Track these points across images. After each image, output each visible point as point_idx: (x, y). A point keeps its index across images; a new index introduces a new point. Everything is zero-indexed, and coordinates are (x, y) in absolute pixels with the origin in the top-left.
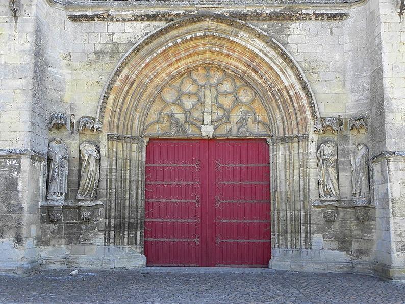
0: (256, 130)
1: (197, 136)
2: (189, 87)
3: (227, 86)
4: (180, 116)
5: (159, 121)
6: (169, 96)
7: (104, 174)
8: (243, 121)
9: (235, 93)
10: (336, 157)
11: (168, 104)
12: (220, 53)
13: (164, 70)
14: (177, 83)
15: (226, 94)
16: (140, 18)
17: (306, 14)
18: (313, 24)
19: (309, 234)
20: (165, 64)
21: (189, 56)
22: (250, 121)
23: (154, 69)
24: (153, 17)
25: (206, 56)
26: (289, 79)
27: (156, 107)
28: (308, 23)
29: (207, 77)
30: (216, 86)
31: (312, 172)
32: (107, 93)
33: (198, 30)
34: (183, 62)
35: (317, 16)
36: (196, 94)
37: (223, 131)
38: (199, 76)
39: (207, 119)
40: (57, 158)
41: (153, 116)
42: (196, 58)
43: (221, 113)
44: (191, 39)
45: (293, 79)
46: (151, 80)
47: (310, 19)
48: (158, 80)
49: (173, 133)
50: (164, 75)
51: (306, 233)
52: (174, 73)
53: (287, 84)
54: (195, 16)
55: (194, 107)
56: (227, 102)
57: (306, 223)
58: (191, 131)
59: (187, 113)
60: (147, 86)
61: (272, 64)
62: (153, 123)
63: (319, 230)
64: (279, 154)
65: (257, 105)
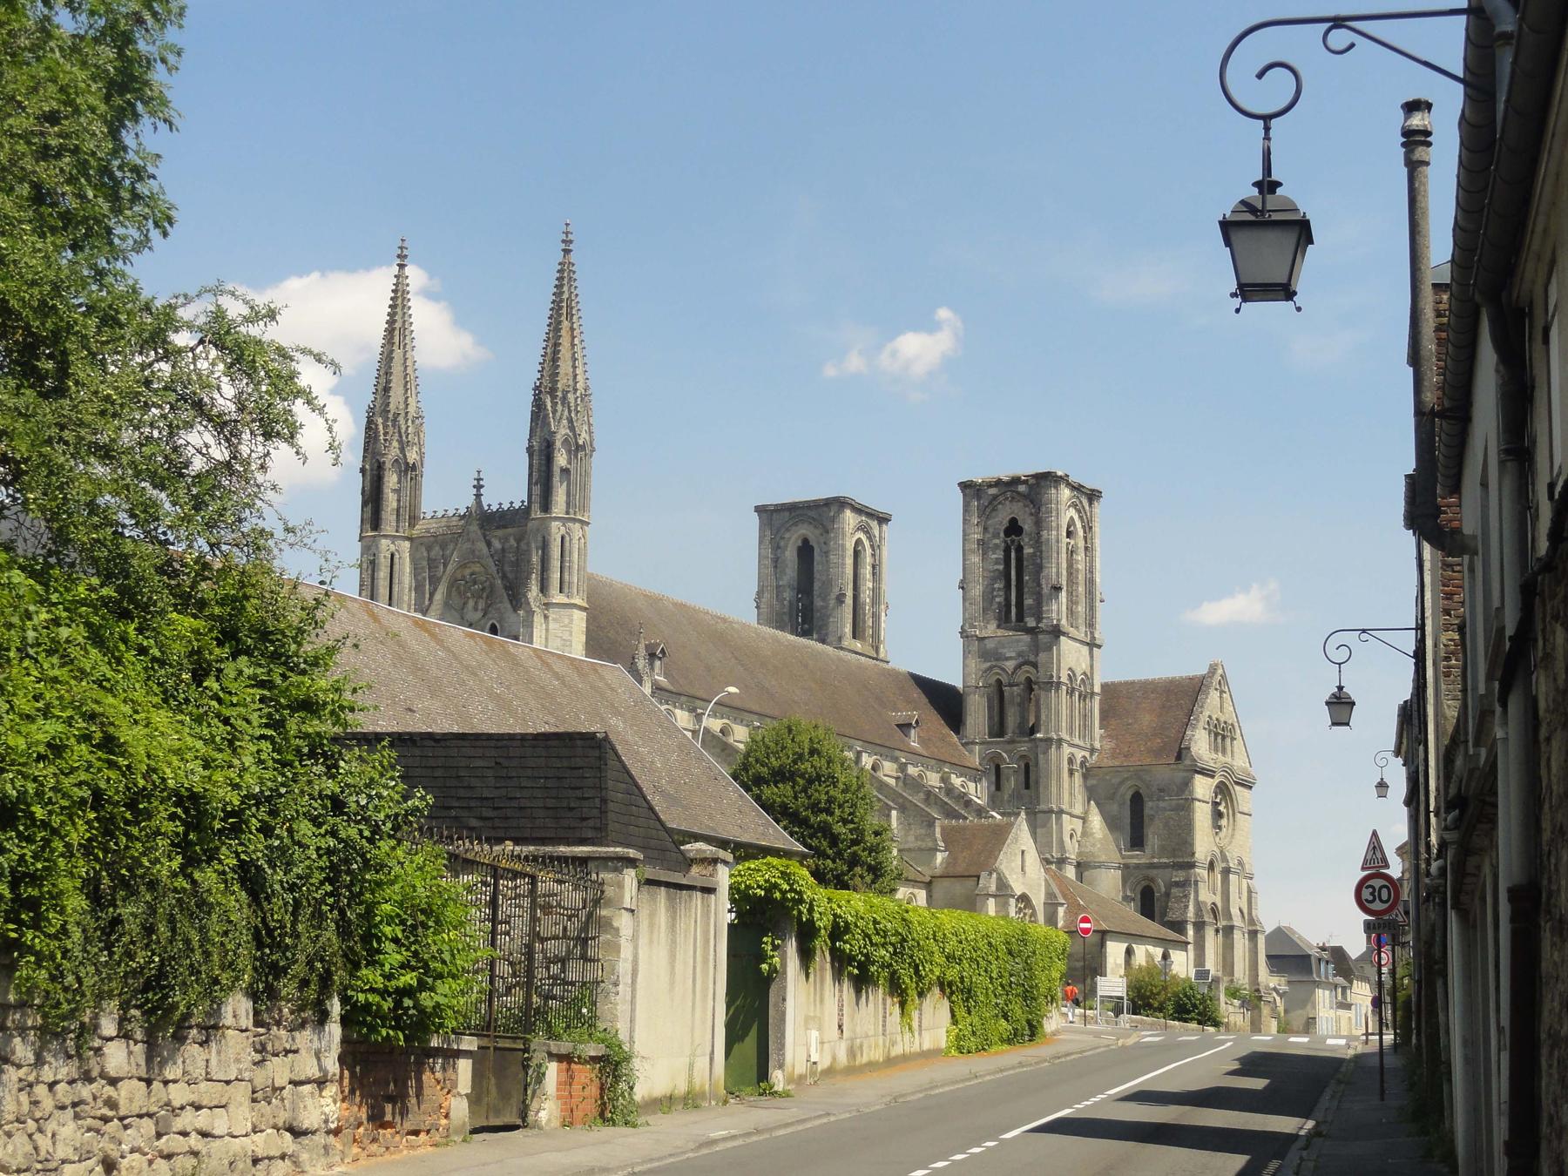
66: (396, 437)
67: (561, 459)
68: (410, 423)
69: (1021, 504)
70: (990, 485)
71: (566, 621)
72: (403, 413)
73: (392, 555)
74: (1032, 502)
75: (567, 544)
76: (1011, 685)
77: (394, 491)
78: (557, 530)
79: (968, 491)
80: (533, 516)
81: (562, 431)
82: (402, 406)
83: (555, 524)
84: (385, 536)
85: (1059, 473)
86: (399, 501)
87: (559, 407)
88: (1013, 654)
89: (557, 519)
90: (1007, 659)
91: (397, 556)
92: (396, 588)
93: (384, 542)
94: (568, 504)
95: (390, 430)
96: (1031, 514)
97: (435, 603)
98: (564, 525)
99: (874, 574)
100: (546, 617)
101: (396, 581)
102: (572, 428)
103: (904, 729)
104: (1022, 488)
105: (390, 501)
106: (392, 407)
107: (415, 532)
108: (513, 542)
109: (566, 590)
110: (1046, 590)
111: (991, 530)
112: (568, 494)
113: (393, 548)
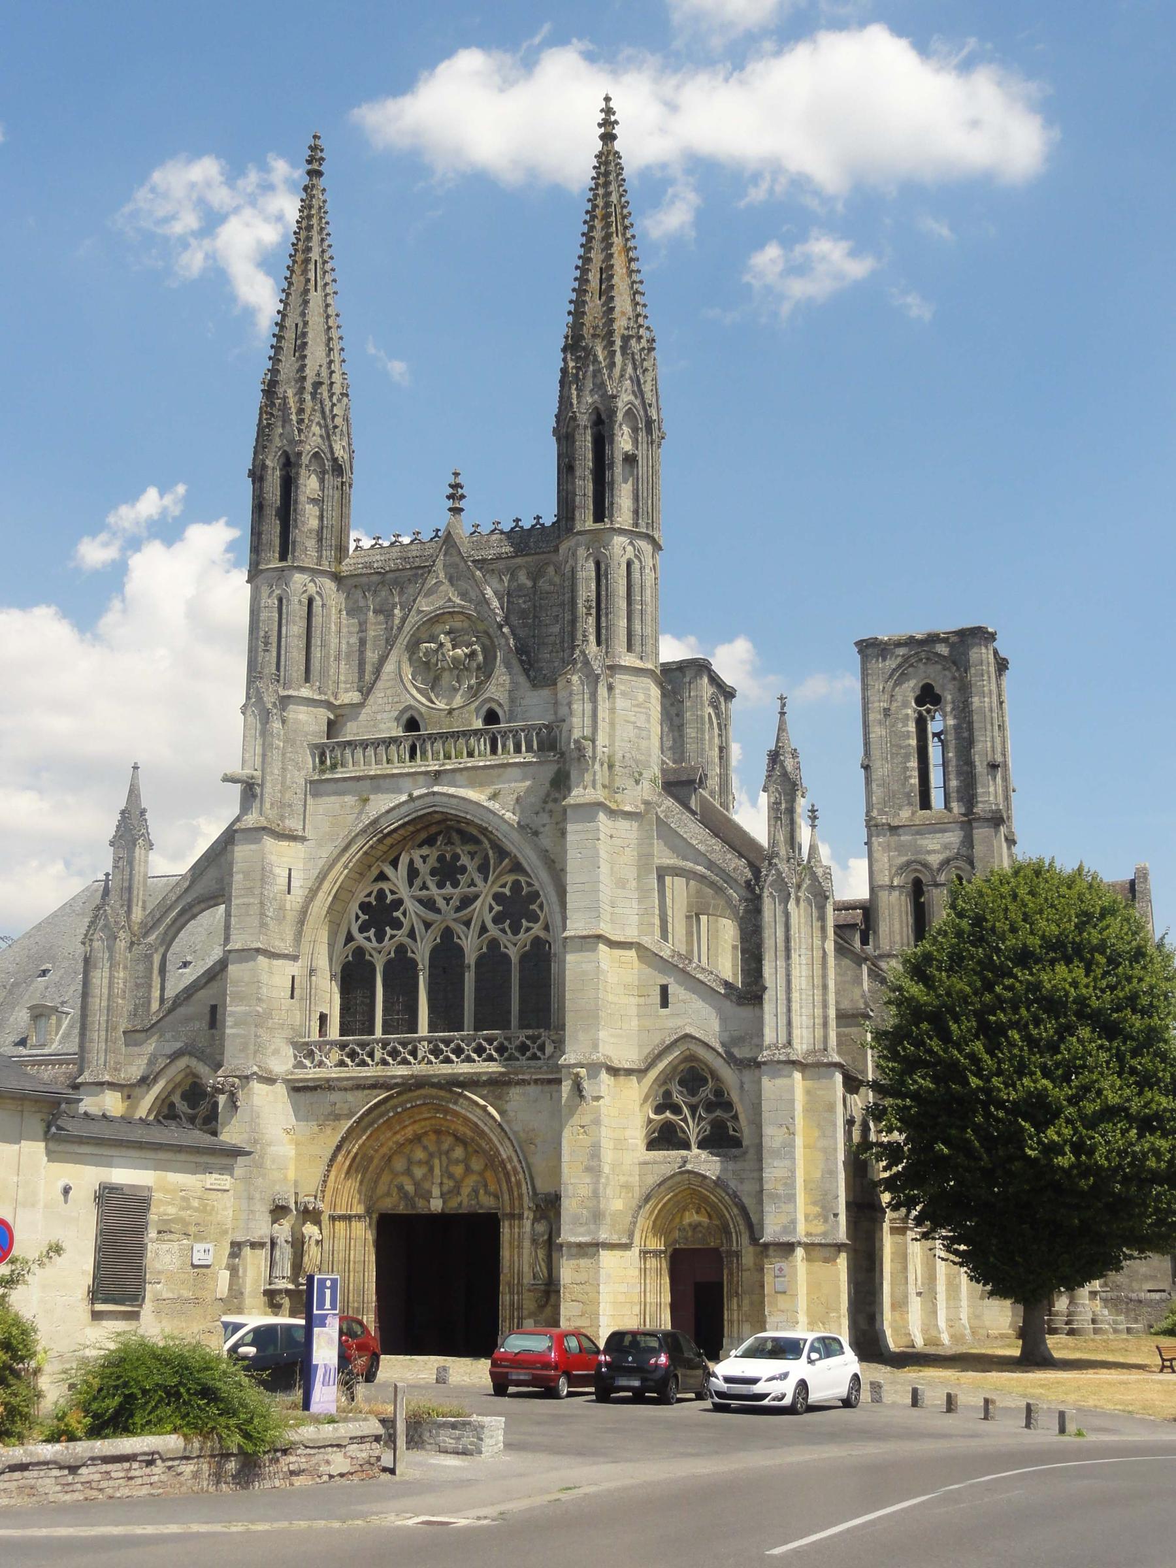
0: (487, 1203)
1: (426, 1211)
2: (420, 1154)
3: (459, 1152)
4: (410, 1188)
5: (388, 1194)
6: (399, 1164)
7: (326, 1255)
8: (475, 1191)
9: (466, 1162)
10: (546, 1237)
11: (396, 1174)
12: (445, 1119)
13: (389, 1139)
14: (407, 1150)
15: (457, 1162)
16: (359, 1087)
17: (523, 1080)
18: (531, 1089)
19: (520, 1319)
20: (389, 1134)
21: (415, 1122)
22: (482, 1192)
23: (377, 1139)
24: (374, 1086)
25: (433, 1122)
26: (505, 1152)
27: (386, 1178)
28: (528, 1088)
29: (439, 1142)
30: (447, 1153)
31: (526, 1252)
32: (328, 1171)
33: (418, 1098)
34: (409, 1128)
35: (536, 1081)
36: (427, 1163)
37: (453, 1204)
38: (430, 1141)
39: (436, 1191)
40: (280, 1241)
41: (382, 1188)
42: (423, 1123)
43: (451, 1184)
44: (412, 1107)
45: (511, 1152)
46: (376, 1151)
47: (529, 1084)
48: (384, 1150)
49: (402, 1209)
50: (390, 1143)
51: (519, 1318)
52: (401, 1141)
53: (504, 1156)
54: (412, 1085)
55: (425, 1176)
56: (458, 1170)
57: (518, 1308)
58: (421, 1207)
59: (417, 1185)
60: (371, 1159)
61: (491, 1135)
62: (382, 1197)
63: (530, 1316)
64: (505, 1230)
65: (489, 1175)
66: (317, 417)
67: (624, 442)
68: (335, 400)
69: (939, 667)
70: (899, 644)
71: (641, 698)
72: (327, 382)
73: (311, 601)
74: (954, 663)
75: (636, 575)
76: (937, 885)
77: (313, 501)
78: (620, 548)
79: (870, 651)
80: (578, 527)
81: (625, 399)
82: (324, 373)
83: (619, 541)
84: (301, 569)
85: (990, 630)
86: (321, 518)
87: (618, 358)
88: (938, 847)
89: (622, 531)
90: (929, 852)
91: (318, 602)
92: (317, 653)
93: (299, 578)
94: (636, 512)
95: (309, 404)
96: (954, 679)
97: (384, 676)
98: (631, 543)
99: (721, 758)
100: (610, 688)
101: (316, 641)
102: (639, 393)
103: (848, 932)
104: (943, 649)
105: (309, 517)
106: (310, 373)
107: (346, 567)
108: (523, 578)
109: (638, 648)
110: (980, 768)
111: (899, 698)
112: (636, 498)
113: (312, 589)
